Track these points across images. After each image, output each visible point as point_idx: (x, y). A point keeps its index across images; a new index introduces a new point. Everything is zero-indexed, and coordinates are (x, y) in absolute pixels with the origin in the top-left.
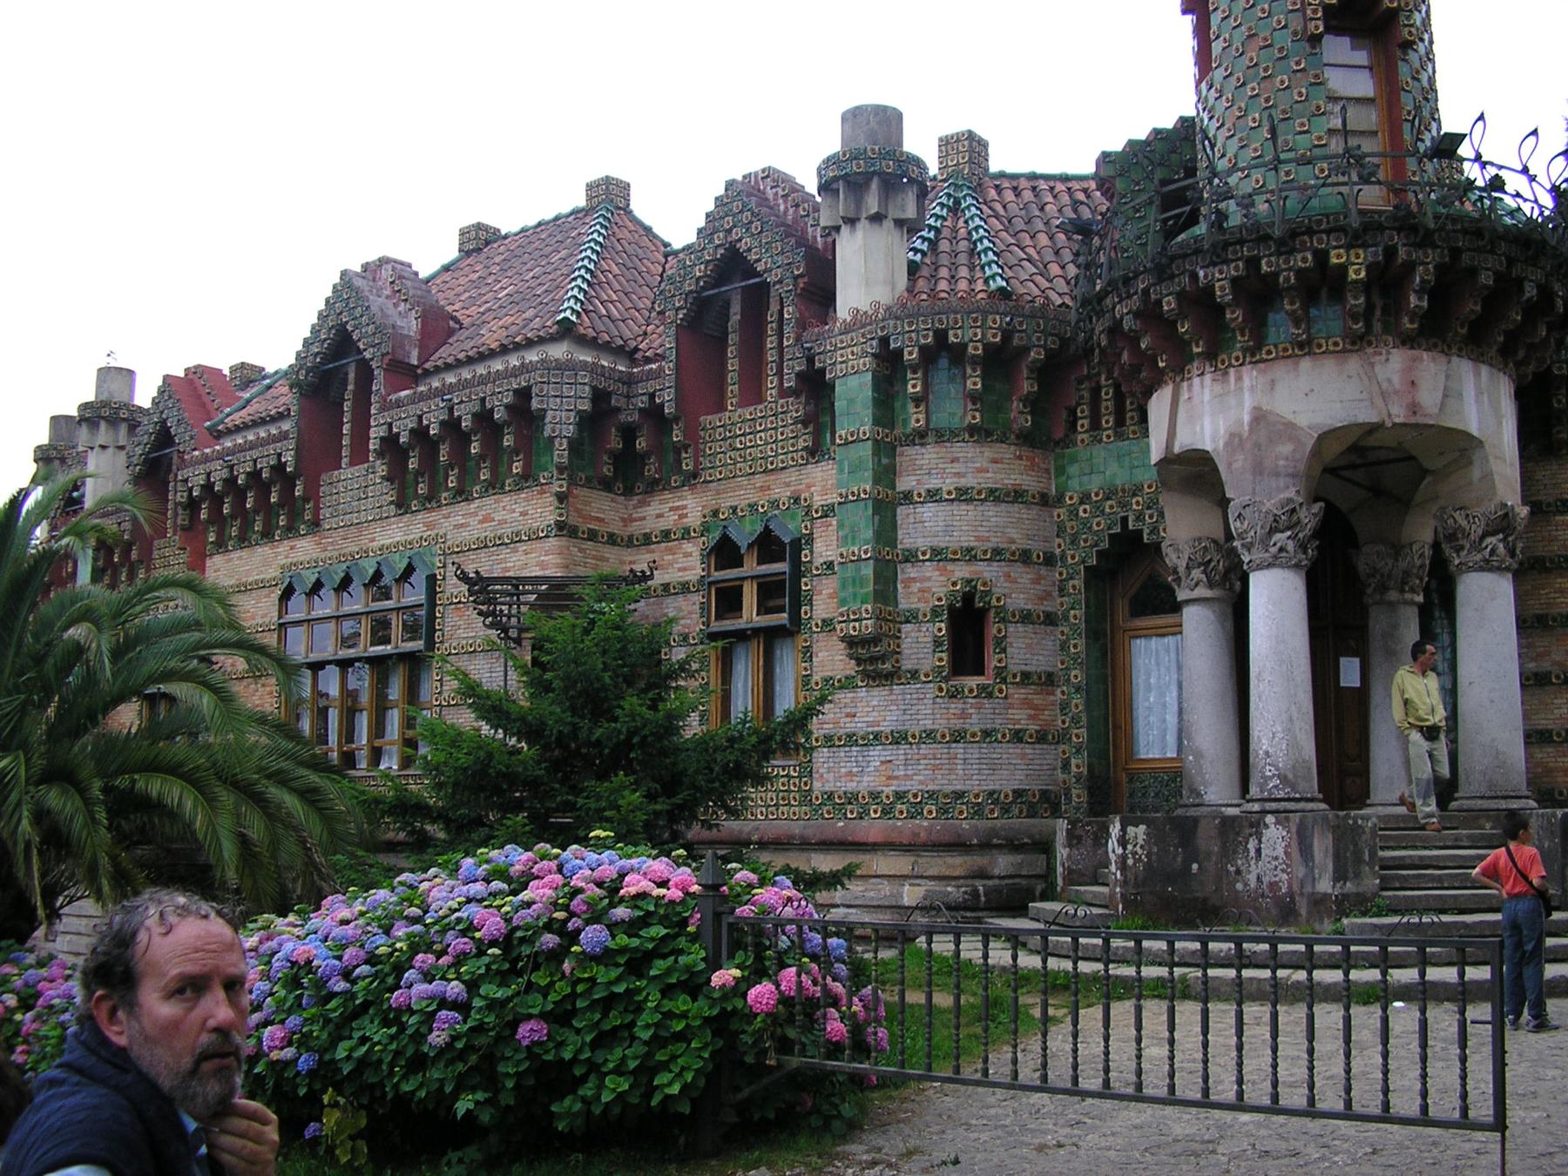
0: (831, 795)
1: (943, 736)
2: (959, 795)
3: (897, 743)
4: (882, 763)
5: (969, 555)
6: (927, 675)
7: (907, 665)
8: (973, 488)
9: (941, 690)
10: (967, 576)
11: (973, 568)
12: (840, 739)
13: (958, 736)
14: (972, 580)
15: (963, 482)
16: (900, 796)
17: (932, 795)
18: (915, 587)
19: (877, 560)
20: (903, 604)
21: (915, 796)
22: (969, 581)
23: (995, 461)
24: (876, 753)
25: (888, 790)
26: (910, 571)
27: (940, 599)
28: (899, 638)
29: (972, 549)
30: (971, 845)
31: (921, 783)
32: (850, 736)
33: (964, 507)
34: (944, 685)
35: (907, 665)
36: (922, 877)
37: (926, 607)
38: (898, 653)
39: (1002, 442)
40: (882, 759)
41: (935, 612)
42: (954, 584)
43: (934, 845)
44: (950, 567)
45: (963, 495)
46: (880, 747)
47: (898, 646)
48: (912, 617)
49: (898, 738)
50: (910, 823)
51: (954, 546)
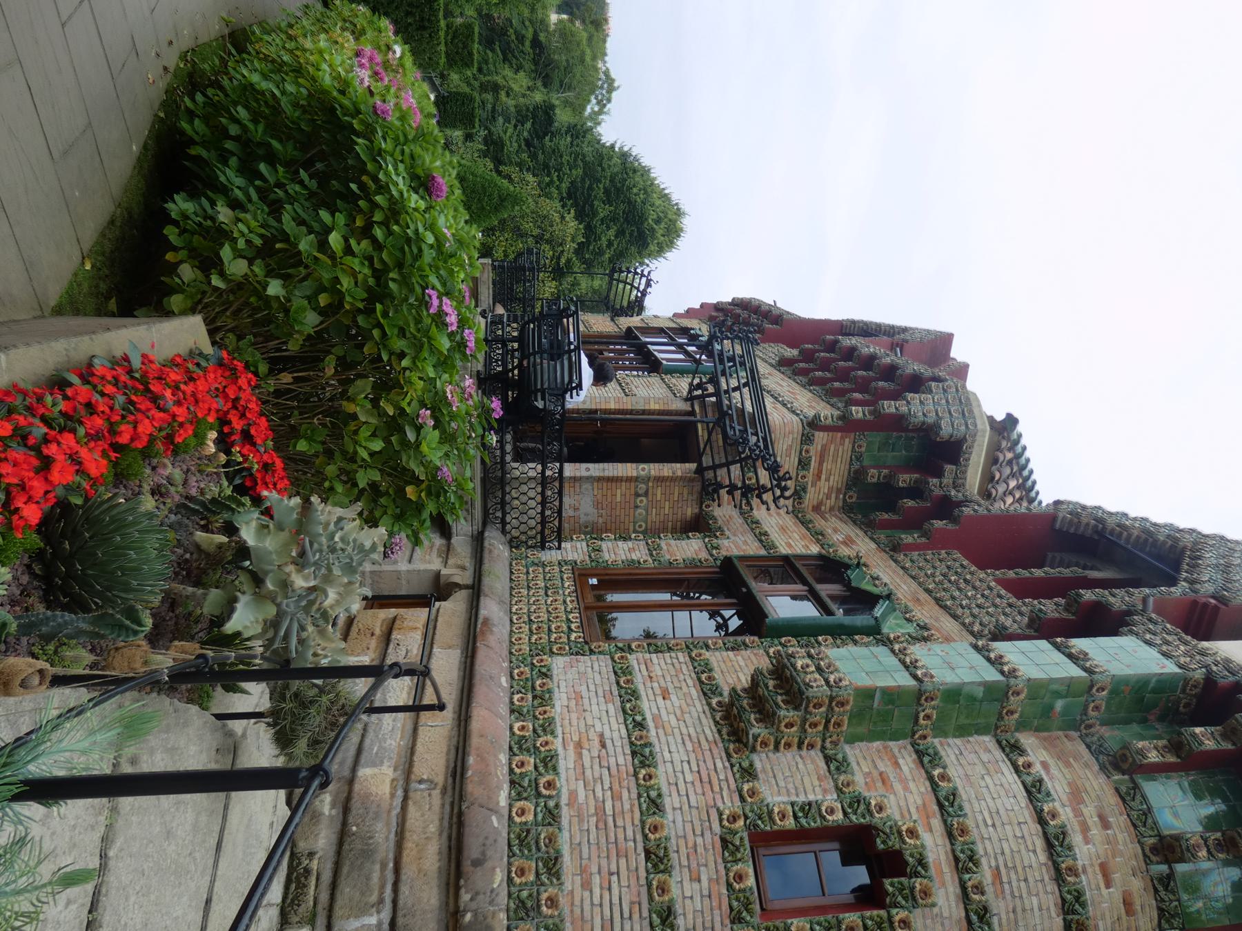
0: (546, 674)
1: (655, 829)
2: (552, 866)
3: (634, 754)
4: (602, 736)
5: (965, 862)
6: (753, 793)
7: (759, 761)
8: (1075, 859)
9: (733, 818)
10: (931, 858)
11: (946, 869)
12: (628, 682)
13: (657, 858)
14: (925, 867)
15: (1076, 839)
16: (549, 762)
17: (552, 816)
18: (884, 766)
19: (919, 696)
20: (853, 753)
21: (549, 785)
22: (921, 862)
23: (1128, 904)
24: (615, 726)
25: (557, 744)
26: (907, 762)
27: (880, 808)
28: (800, 747)
29: (977, 864)
30: (457, 888)
31: (573, 795)
32: (635, 694)
33: (1039, 843)
34: (741, 823)
35: (759, 761)
36: (406, 798)
37: (859, 781)
38: (777, 748)
39: (1161, 911)
40: (607, 734)
41: (857, 800)
42: (912, 833)
43: (460, 814)
44: (936, 823)
45: (1055, 842)
46: (624, 731)
47: (788, 745)
48: (836, 765)
49: (642, 755)
50: (502, 773)
51: (975, 834)
